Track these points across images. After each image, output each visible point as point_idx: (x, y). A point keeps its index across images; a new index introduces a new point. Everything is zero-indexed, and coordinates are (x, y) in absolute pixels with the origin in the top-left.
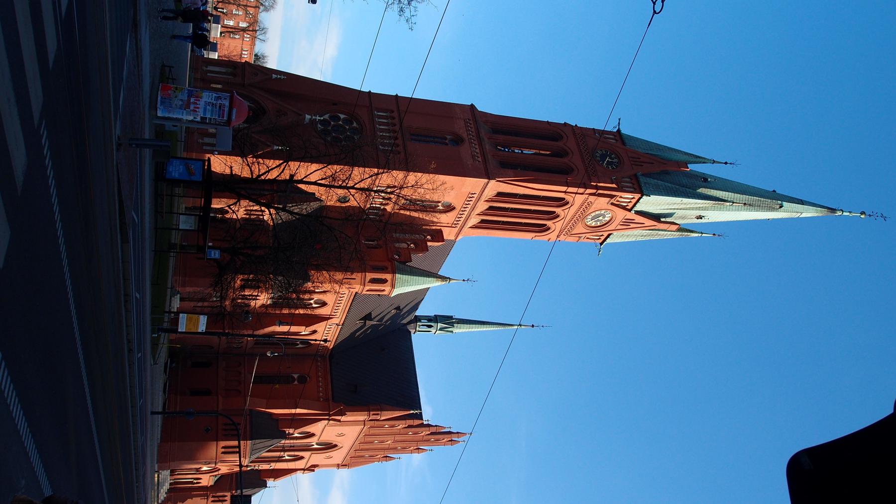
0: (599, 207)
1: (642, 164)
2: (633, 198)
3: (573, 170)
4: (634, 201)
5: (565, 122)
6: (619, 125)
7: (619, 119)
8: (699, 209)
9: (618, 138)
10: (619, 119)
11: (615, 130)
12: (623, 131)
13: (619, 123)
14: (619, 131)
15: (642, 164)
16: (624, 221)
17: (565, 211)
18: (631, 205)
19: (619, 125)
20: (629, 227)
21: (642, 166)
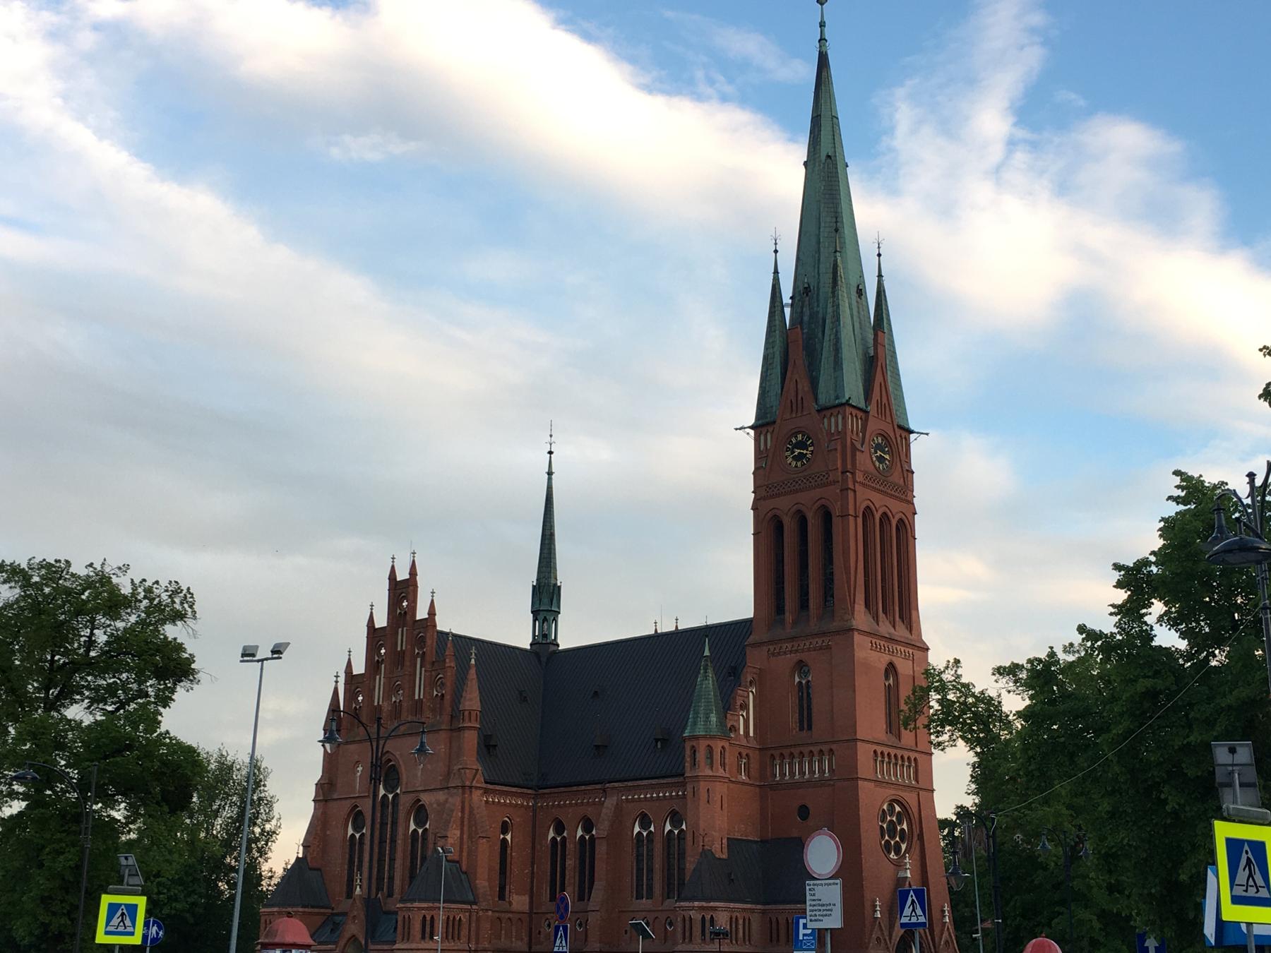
0: (868, 461)
1: (799, 398)
2: (851, 414)
4: (855, 412)
5: (752, 509)
6: (745, 428)
8: (849, 293)
11: (752, 432)
12: (751, 421)
13: (740, 429)
14: (751, 427)
15: (799, 398)
16: (880, 415)
17: (877, 507)
18: (860, 414)
19: (745, 428)
20: (887, 405)
21: (802, 398)
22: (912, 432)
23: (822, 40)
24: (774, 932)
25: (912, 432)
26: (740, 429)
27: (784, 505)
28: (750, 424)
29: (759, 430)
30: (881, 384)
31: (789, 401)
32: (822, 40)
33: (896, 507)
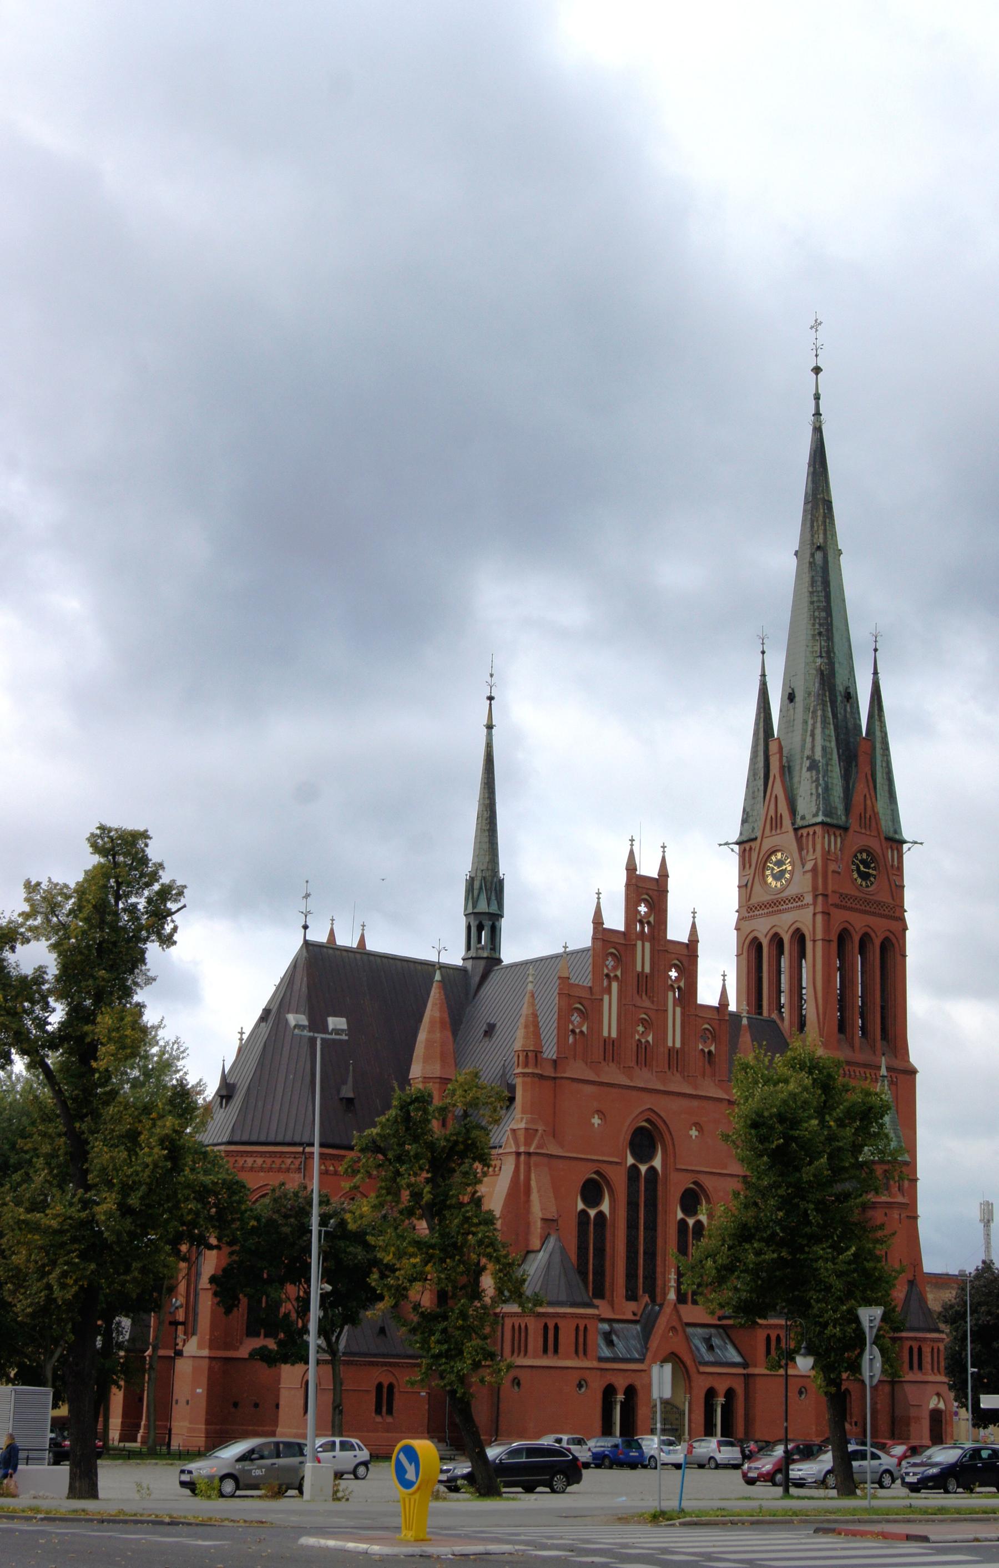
3: (798, 930)
7: (720, 845)
9: (747, 846)
10: (720, 845)
11: (736, 848)
12: (735, 836)
13: (727, 844)
14: (737, 843)
15: (779, 815)
22: (905, 842)
23: (817, 414)
24: (581, 1340)
25: (905, 842)
26: (727, 844)
27: (763, 927)
28: (734, 841)
29: (743, 846)
30: (865, 796)
31: (769, 817)
32: (817, 414)
33: (880, 927)
